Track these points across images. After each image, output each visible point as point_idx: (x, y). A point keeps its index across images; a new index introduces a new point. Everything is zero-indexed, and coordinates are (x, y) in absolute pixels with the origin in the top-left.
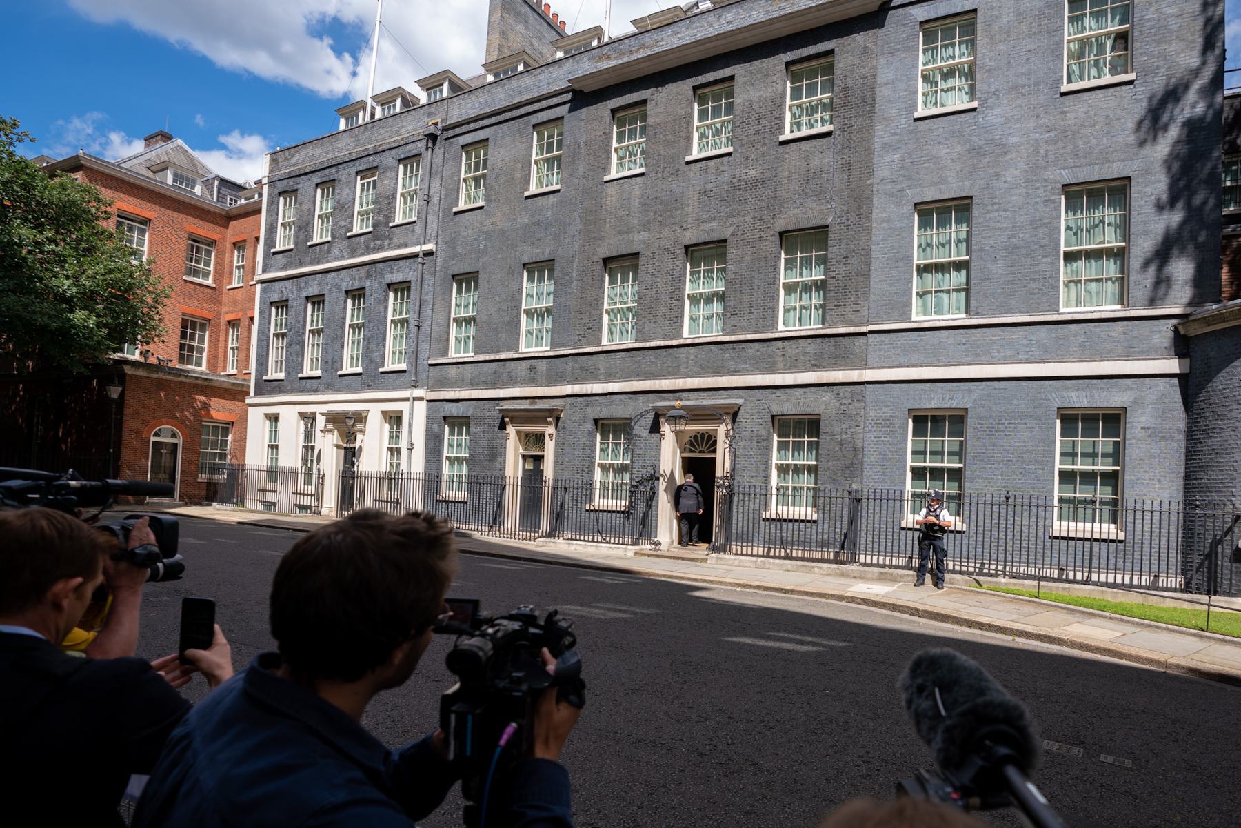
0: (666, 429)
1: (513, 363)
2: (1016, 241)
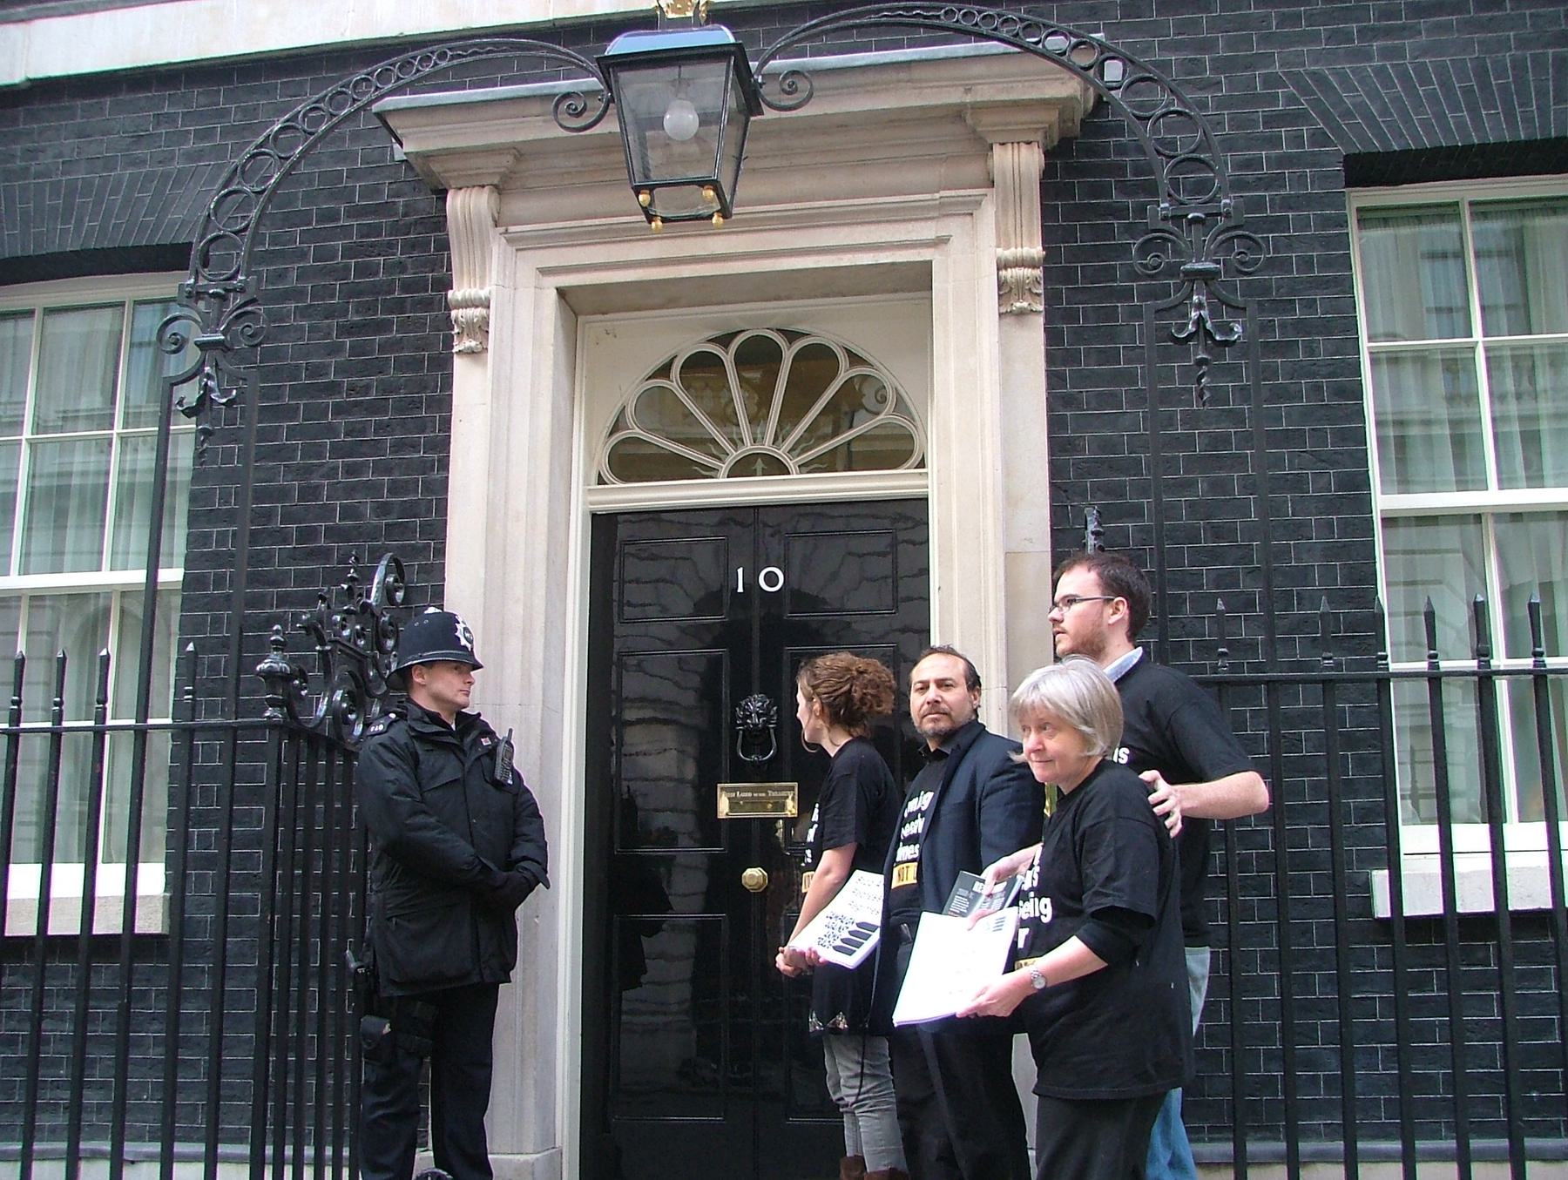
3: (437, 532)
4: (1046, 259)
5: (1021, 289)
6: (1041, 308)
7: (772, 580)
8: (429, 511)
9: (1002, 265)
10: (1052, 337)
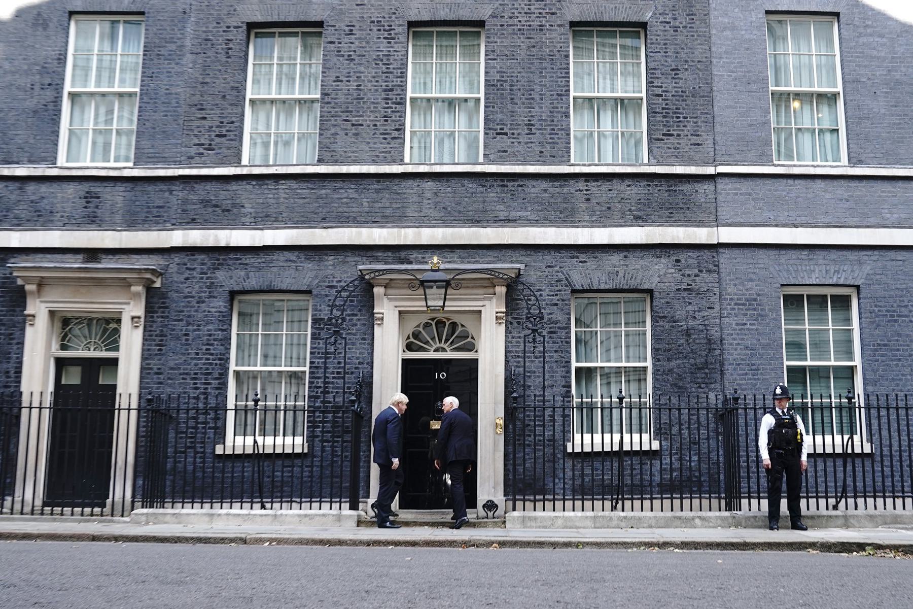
0: (387, 309)
1: (44, 188)
2: (898, 75)
5: (501, 318)
7: (443, 375)
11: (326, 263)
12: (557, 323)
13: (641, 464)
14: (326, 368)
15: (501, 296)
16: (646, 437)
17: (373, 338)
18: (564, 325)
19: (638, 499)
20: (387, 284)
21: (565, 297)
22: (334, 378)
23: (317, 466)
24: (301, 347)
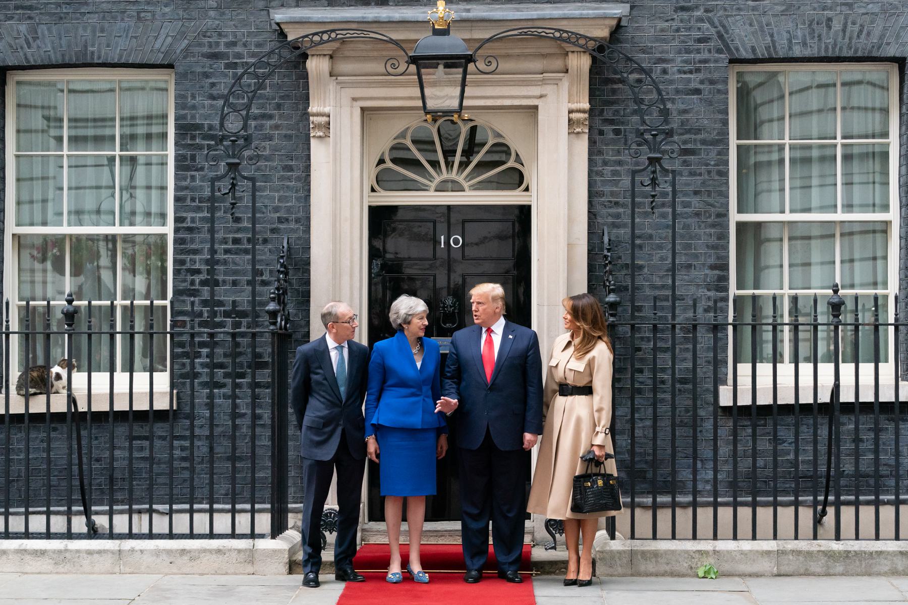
0: (334, 104)
3: (305, 222)
4: (590, 109)
5: (579, 122)
6: (587, 131)
7: (456, 242)
8: (299, 211)
9: (570, 112)
10: (592, 142)
11: (202, 4)
12: (698, 131)
13: (877, 431)
14: (212, 231)
15: (579, 75)
16: (887, 370)
17: (308, 168)
18: (714, 135)
19: (868, 503)
20: (334, 51)
21: (716, 76)
22: (227, 251)
23: (200, 438)
24: (154, 193)
